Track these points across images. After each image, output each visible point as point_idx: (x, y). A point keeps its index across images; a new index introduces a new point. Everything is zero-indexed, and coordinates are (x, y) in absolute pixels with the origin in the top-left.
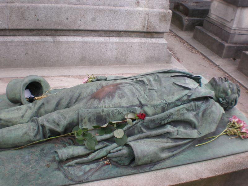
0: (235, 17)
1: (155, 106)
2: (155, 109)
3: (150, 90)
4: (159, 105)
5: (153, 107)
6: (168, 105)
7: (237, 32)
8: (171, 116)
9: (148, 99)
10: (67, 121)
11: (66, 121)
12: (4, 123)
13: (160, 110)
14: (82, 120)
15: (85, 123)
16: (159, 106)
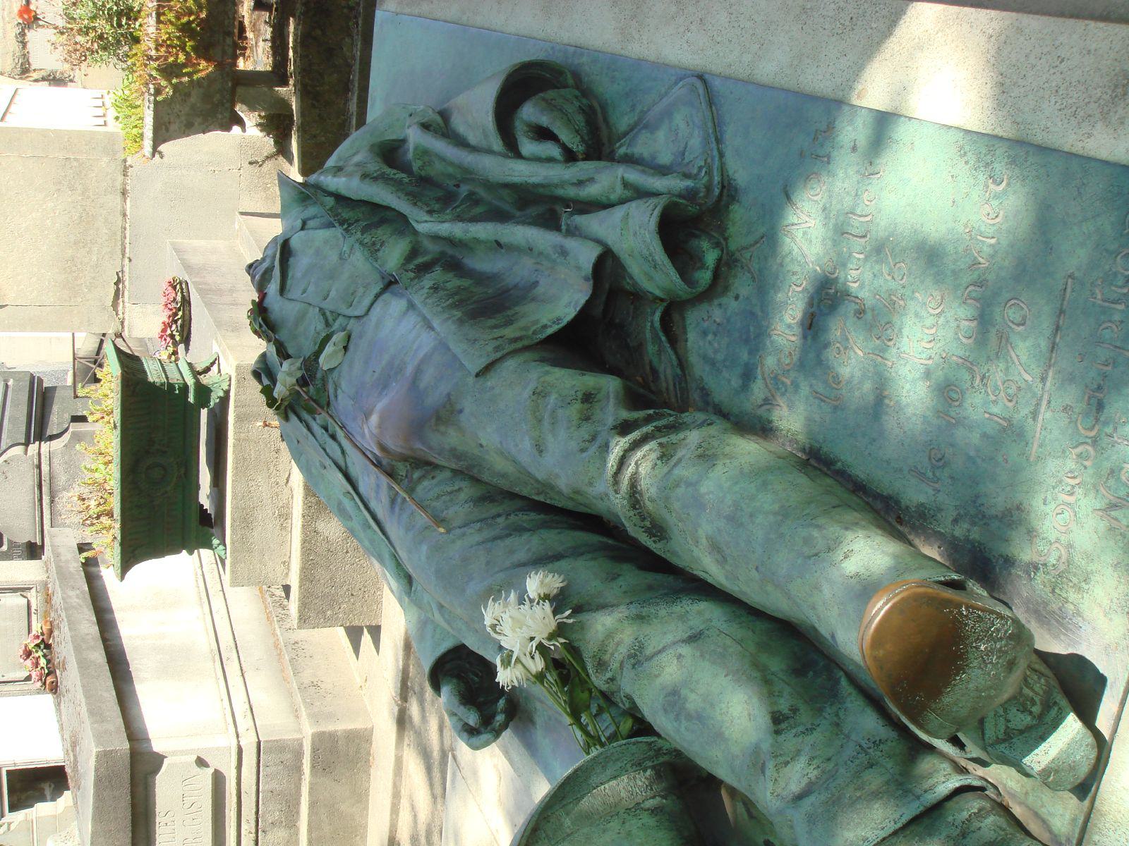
0: (183, 753)
1: (373, 250)
2: (381, 246)
3: (330, 319)
4: (361, 243)
5: (380, 254)
6: (350, 225)
7: (244, 723)
8: (375, 175)
9: (361, 290)
10: (547, 373)
11: (548, 378)
12: (787, 690)
13: (379, 232)
14: (516, 340)
15: (526, 328)
16: (366, 241)
